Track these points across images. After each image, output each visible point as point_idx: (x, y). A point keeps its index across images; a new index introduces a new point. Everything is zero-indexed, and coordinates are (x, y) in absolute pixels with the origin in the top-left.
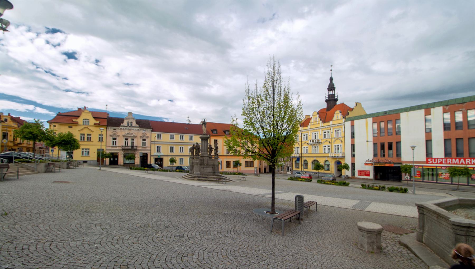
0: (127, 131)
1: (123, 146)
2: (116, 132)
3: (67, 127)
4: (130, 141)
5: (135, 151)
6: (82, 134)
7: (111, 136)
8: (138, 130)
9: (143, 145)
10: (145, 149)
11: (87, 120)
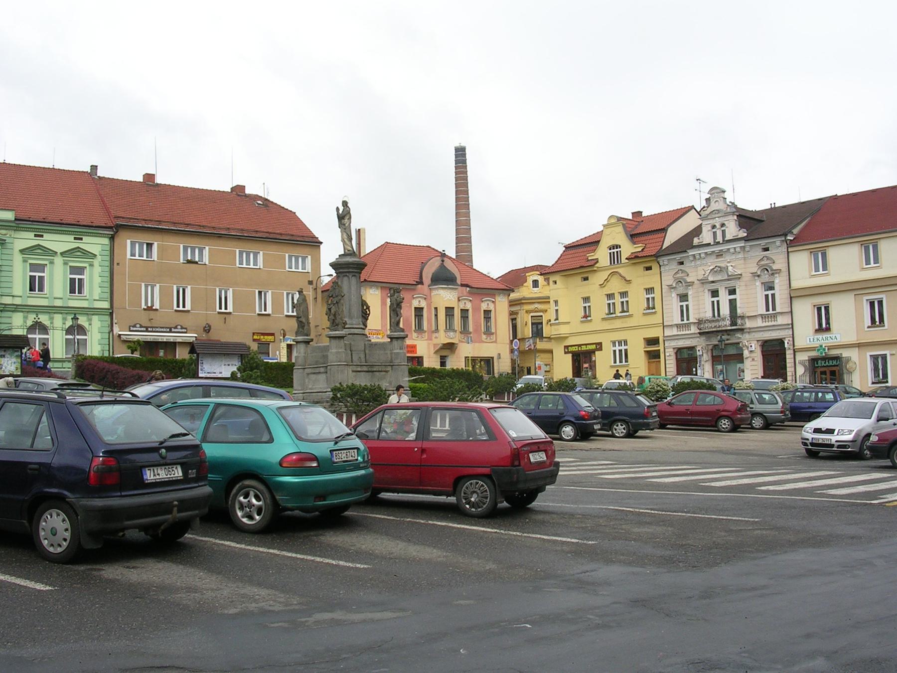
0: (711, 263)
1: (700, 322)
2: (683, 271)
3: (578, 279)
4: (724, 298)
5: (739, 335)
6: (610, 296)
7: (671, 287)
8: (743, 248)
9: (768, 310)
10: (773, 323)
11: (618, 246)
